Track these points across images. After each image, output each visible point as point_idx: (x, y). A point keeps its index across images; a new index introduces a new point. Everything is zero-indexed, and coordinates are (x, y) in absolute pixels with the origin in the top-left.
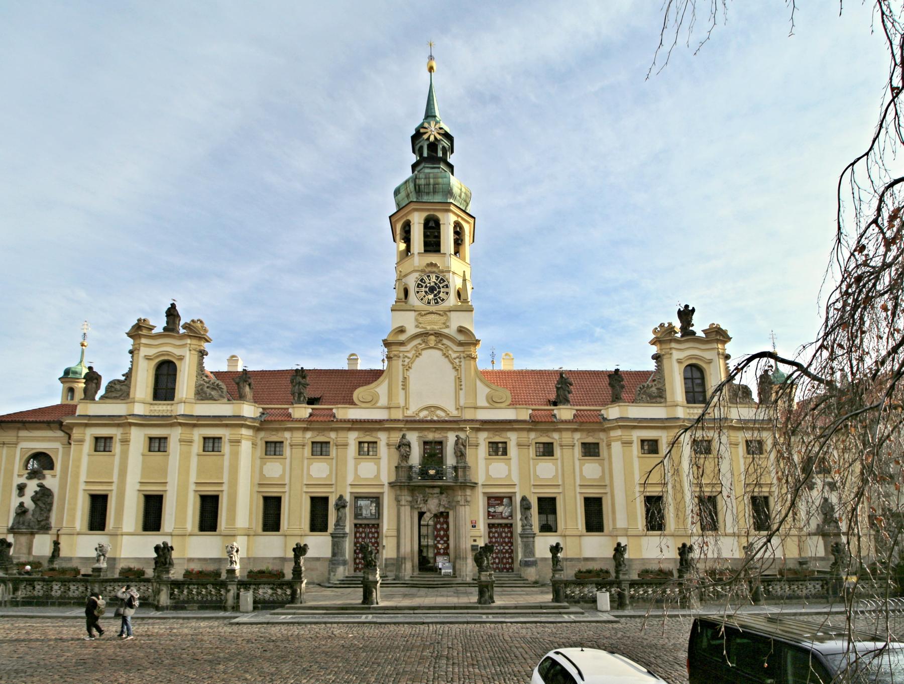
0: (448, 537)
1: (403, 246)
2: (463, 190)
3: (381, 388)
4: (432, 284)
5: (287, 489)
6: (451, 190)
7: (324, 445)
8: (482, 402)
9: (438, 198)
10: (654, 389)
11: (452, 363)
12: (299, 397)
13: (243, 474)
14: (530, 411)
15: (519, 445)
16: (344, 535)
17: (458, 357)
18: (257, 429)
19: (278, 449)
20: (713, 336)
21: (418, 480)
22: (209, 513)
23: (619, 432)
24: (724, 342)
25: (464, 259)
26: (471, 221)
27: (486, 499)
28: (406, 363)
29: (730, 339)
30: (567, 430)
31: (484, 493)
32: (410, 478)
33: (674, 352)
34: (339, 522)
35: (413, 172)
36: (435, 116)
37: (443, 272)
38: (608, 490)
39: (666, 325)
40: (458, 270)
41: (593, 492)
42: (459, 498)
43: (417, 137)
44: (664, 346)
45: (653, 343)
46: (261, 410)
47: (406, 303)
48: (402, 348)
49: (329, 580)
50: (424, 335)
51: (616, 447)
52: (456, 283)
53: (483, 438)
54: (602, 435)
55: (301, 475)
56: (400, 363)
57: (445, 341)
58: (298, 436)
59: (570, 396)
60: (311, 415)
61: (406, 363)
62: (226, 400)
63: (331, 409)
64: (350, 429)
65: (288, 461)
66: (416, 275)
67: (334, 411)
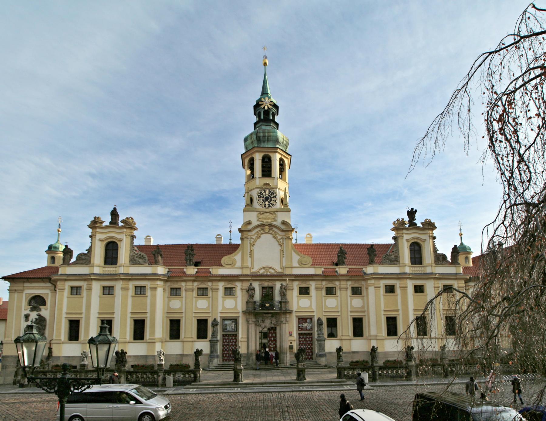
0: (276, 341)
1: (249, 172)
2: (285, 139)
3: (237, 257)
4: (267, 196)
5: (183, 315)
6: (278, 139)
7: (204, 290)
9: (270, 145)
10: (393, 256)
12: (190, 262)
13: (159, 306)
14: (323, 269)
16: (217, 341)
17: (282, 238)
18: (166, 281)
19: (178, 292)
20: (427, 226)
21: (259, 310)
22: (139, 330)
23: (373, 281)
24: (433, 230)
25: (285, 180)
26: (289, 157)
27: (297, 319)
28: (252, 242)
29: (436, 228)
31: (296, 316)
32: (255, 309)
33: (405, 235)
34: (214, 334)
35: (255, 128)
36: (268, 94)
37: (273, 188)
38: (366, 313)
39: (401, 220)
40: (282, 187)
42: (283, 319)
43: (257, 106)
44: (399, 232)
45: (393, 230)
46: (168, 270)
47: (251, 206)
49: (209, 367)
50: (262, 226)
51: (371, 290)
52: (281, 194)
53: (296, 285)
54: (363, 283)
55: (193, 306)
57: (274, 229)
58: (190, 285)
59: (345, 260)
60: (197, 272)
61: (252, 242)
62: (147, 265)
63: (209, 269)
64: (219, 281)
65: (184, 299)
66: (258, 190)
67: (210, 270)
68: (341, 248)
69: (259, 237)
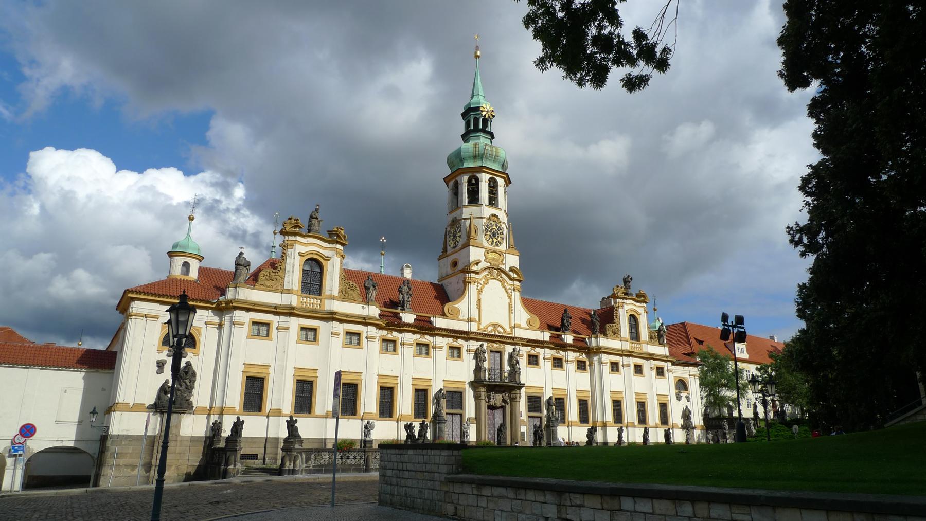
8: (524, 325)
41: (584, 396)
53: (524, 351)
57: (503, 275)
68: (566, 311)
69: (486, 283)
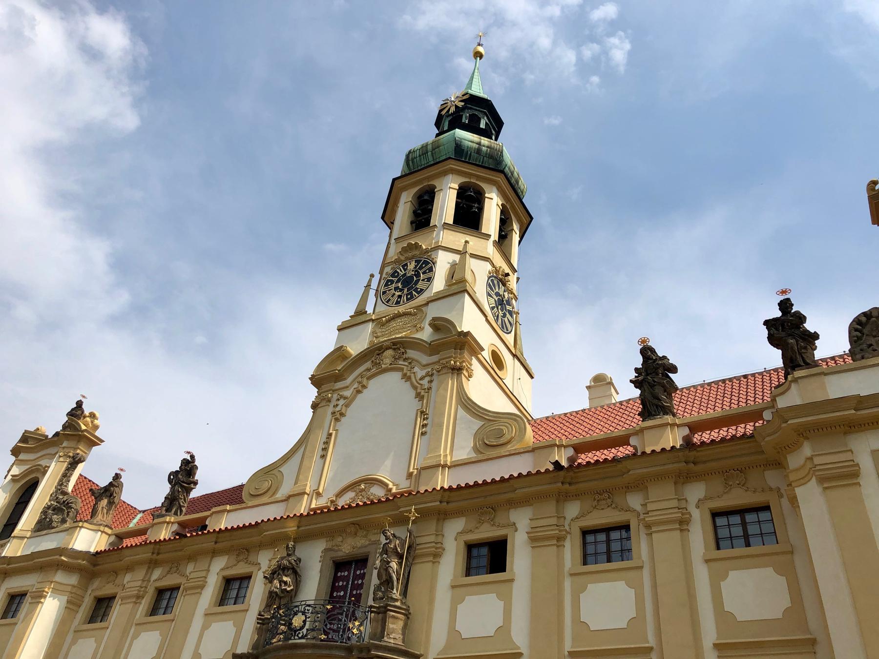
8: (464, 451)
11: (415, 388)
15: (535, 540)
17: (427, 375)
30: (659, 477)
48: (339, 385)
56: (330, 409)
57: (411, 353)
